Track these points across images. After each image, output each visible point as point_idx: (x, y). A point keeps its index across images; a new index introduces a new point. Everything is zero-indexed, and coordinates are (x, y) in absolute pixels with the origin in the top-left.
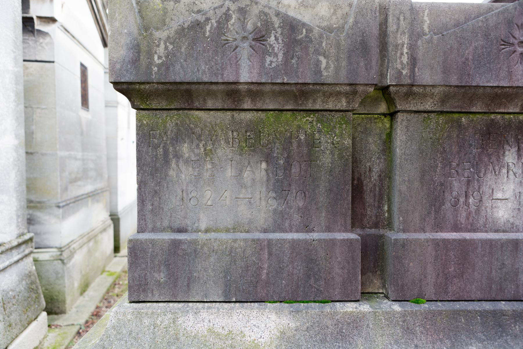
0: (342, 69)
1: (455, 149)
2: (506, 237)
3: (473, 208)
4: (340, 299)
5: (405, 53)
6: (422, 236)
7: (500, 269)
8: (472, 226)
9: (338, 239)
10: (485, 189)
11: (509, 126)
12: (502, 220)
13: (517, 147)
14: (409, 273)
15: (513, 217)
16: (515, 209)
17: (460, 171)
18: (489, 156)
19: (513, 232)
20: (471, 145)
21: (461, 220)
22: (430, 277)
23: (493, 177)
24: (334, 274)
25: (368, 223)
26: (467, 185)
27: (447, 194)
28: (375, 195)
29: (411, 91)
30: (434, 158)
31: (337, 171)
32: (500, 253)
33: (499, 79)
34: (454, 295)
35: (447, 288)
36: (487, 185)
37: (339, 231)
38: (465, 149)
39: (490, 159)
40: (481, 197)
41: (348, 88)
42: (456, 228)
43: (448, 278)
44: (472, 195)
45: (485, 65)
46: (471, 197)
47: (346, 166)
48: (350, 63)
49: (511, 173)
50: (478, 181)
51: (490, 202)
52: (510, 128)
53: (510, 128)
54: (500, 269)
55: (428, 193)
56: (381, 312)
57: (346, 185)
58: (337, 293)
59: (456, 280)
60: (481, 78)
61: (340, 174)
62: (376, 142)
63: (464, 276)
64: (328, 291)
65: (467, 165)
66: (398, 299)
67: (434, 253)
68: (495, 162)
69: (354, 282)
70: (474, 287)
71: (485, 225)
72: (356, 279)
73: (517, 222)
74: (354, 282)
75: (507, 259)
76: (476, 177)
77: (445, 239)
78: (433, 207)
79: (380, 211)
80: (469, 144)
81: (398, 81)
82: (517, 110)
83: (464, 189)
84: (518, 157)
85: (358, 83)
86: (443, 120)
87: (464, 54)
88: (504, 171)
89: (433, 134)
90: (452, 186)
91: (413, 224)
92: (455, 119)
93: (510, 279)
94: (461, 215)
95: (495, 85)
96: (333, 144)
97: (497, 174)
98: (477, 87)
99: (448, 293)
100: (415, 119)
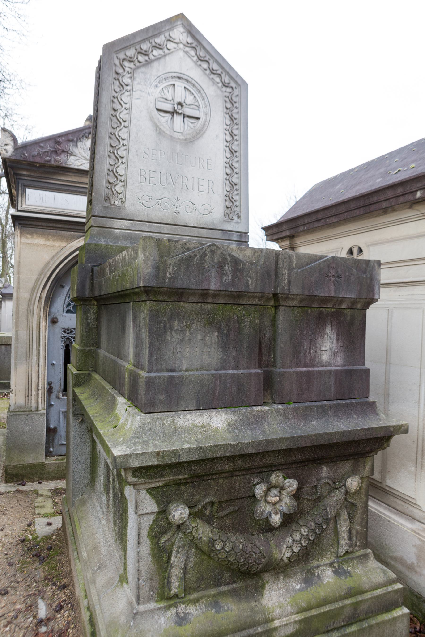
6: (291, 370)
10: (318, 345)
17: (307, 336)
18: (320, 329)
20: (312, 323)
27: (301, 348)
28: (267, 350)
29: (288, 297)
37: (253, 369)
42: (305, 366)
49: (328, 337)
50: (315, 341)
73: (331, 362)
82: (331, 307)
83: (309, 345)
88: (326, 336)
97: (323, 338)
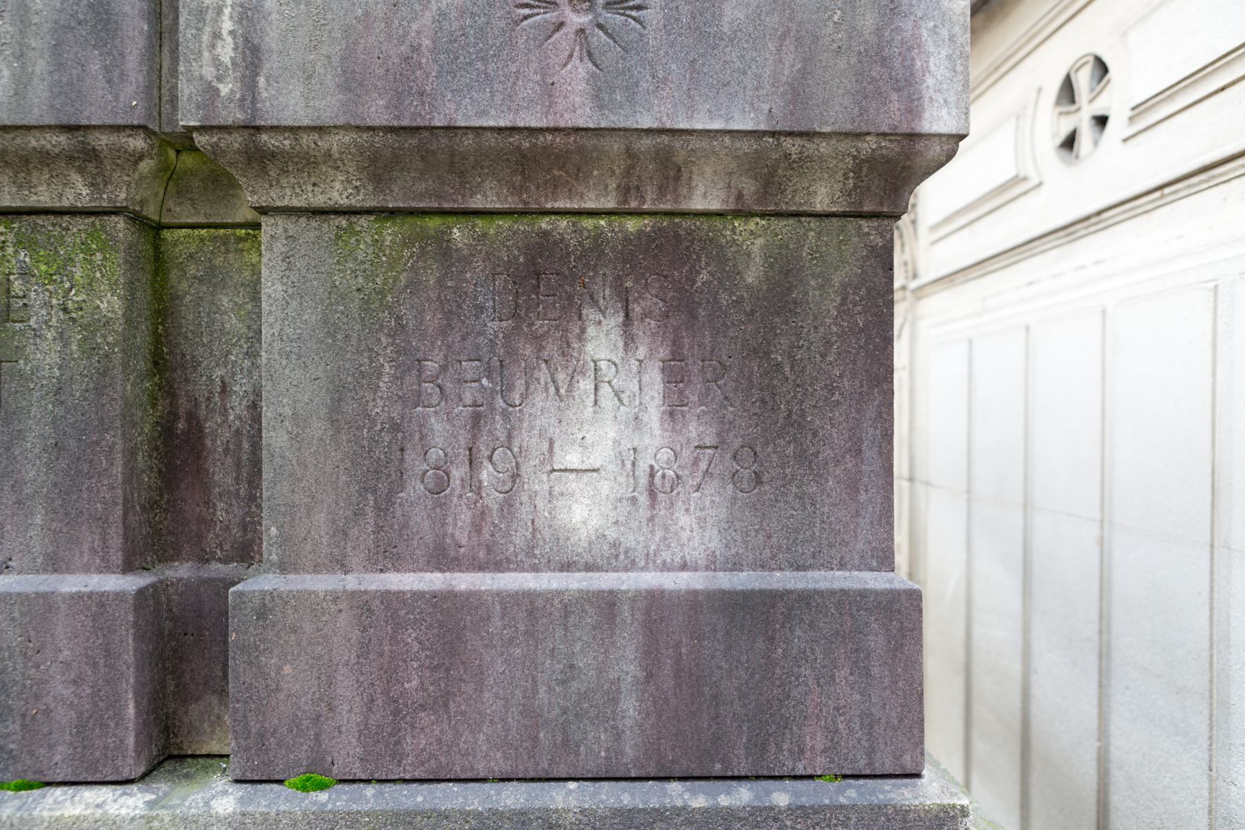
0: (36, 81)
1: (433, 320)
2: (584, 585)
3: (492, 498)
4: (69, 778)
5: (225, 33)
6: (322, 583)
7: (563, 682)
8: (489, 550)
9: (60, 594)
10: (526, 438)
11: (596, 247)
12: (583, 534)
13: (622, 314)
14: (282, 696)
15: (616, 523)
16: (620, 500)
17: (449, 386)
18: (538, 340)
19: (616, 570)
20: (480, 309)
21: (457, 534)
22: (346, 707)
23: (552, 404)
24: (49, 699)
25: (220, 545)
26: (473, 428)
27: (410, 456)
28: (238, 464)
29: (260, 148)
30: (370, 350)
31: (77, 389)
32: (559, 632)
33: (514, 106)
34: (422, 763)
35: (398, 743)
36: (532, 428)
37: (86, 569)
38: (463, 322)
39: (541, 348)
40: (517, 464)
41: (63, 139)
42: (442, 559)
43: (400, 712)
44: (490, 458)
45: (470, 64)
46: (486, 463)
47: (105, 373)
48: (59, 65)
49: (605, 390)
50: (505, 415)
51: (545, 477)
52: (599, 258)
53: (599, 258)
54: (563, 682)
55: (355, 453)
56: (167, 819)
57: (107, 431)
58: (59, 760)
59: (425, 718)
60: (459, 104)
61: (86, 399)
62: (241, 307)
63: (452, 704)
64: (32, 754)
65: (470, 368)
66: (249, 776)
67: (356, 634)
68: (557, 358)
69: (112, 724)
70: (482, 737)
71: (530, 550)
72: (119, 717)
73: (630, 540)
74: (112, 724)
75: (582, 651)
76: (500, 403)
77: (388, 592)
78: (370, 496)
79: (254, 509)
80: (476, 307)
81: (206, 117)
82: (610, 203)
83: (463, 439)
84: (626, 344)
85: (85, 122)
86: (395, 234)
87: (405, 35)
88: (586, 385)
89: (366, 278)
90: (425, 431)
91: (308, 547)
92: (432, 232)
93: (593, 713)
94: (455, 519)
95: (502, 124)
96: (65, 310)
97: (564, 396)
98: (451, 129)
99: (403, 756)
100: (312, 235)
